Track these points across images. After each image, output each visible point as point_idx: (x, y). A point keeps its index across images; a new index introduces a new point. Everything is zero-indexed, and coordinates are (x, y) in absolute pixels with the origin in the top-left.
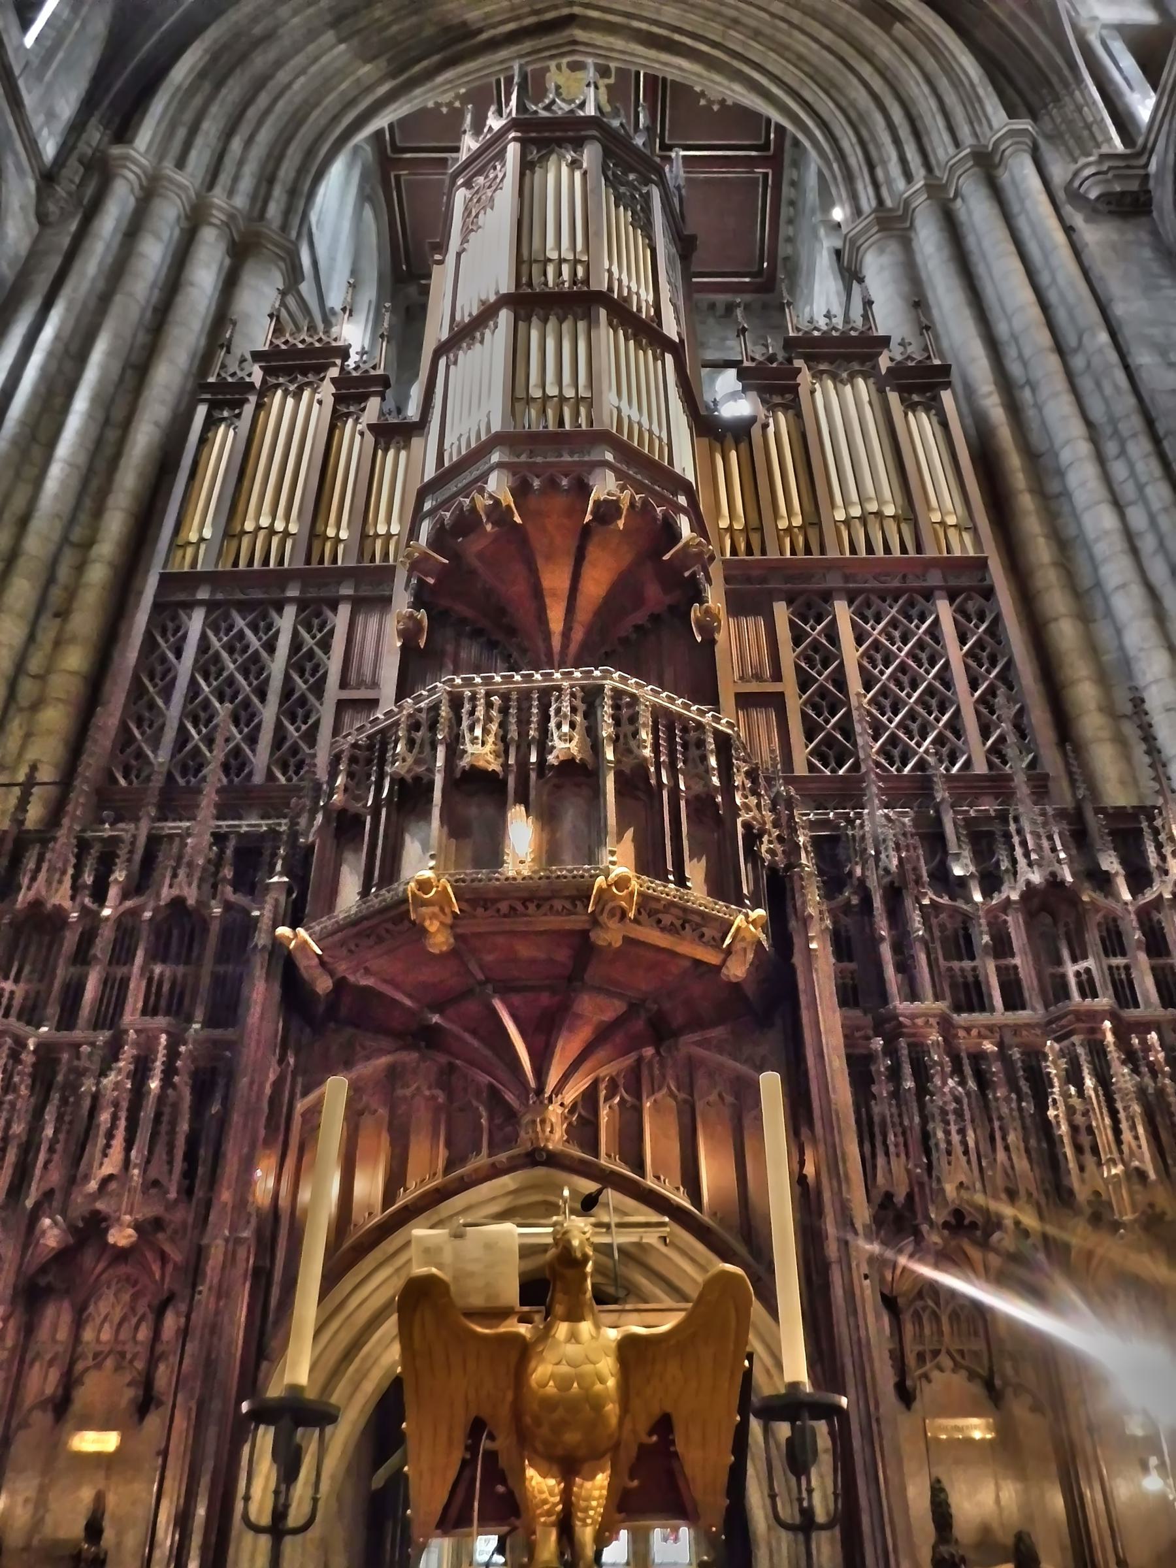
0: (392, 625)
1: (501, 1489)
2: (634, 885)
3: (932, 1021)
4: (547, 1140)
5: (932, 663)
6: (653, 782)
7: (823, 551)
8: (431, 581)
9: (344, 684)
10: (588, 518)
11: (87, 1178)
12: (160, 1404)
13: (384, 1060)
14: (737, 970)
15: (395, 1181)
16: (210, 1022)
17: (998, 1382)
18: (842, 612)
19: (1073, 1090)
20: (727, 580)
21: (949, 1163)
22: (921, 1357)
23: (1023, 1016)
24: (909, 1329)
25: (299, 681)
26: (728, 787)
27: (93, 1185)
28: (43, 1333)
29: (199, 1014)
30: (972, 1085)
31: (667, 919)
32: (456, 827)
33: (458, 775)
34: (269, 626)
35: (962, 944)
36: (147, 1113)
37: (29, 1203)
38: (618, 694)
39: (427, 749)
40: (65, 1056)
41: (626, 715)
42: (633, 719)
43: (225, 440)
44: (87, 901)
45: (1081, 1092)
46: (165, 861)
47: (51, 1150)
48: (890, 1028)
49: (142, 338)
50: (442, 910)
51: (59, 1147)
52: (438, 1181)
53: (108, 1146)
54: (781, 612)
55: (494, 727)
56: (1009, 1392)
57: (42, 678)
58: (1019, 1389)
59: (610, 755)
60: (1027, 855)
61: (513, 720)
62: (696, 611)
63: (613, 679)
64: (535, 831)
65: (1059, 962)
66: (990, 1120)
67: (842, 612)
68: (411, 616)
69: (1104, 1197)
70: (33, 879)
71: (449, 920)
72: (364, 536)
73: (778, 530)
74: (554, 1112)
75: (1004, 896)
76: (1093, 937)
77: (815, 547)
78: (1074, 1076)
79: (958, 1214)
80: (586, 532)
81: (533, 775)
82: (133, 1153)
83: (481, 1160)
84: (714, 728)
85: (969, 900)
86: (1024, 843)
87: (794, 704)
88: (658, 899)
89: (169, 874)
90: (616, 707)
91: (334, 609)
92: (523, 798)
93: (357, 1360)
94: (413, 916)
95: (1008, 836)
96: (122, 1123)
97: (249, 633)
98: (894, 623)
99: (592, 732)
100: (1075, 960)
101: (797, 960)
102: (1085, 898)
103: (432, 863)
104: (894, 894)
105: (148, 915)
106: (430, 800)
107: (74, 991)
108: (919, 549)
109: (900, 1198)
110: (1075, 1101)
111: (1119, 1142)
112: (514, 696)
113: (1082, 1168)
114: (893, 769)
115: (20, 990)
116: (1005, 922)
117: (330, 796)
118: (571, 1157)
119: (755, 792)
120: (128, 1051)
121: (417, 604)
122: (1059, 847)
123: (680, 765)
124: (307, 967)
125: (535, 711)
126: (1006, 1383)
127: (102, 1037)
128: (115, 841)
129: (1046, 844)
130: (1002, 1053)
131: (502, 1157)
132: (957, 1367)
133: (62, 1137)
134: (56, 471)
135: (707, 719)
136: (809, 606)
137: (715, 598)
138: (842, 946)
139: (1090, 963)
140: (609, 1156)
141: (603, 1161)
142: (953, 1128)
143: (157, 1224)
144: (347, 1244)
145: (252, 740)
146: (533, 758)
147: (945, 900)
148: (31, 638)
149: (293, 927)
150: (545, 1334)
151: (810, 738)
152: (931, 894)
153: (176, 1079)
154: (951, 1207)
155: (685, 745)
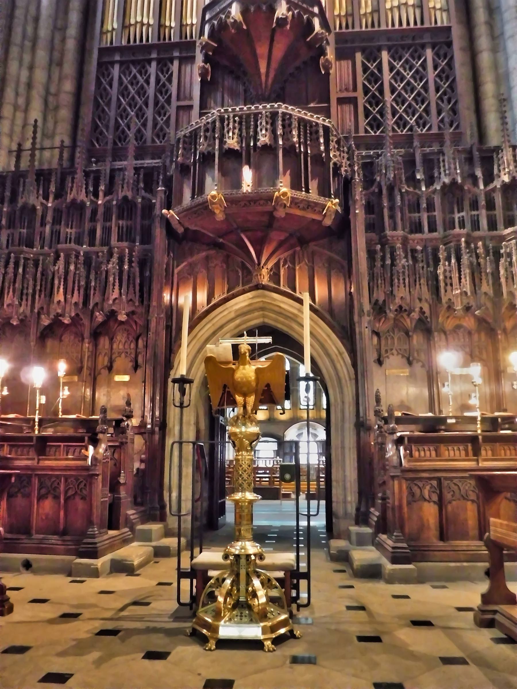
0: (196, 72)
1: (232, 398)
2: (289, 195)
3: (400, 238)
4: (262, 281)
5: (421, 80)
6: (297, 151)
7: (379, 26)
8: (211, 53)
9: (178, 99)
10: (274, 25)
11: (108, 299)
12: (141, 367)
13: (204, 254)
14: (328, 222)
15: (210, 296)
16: (142, 242)
17: (411, 359)
18: (385, 56)
19: (447, 263)
20: (337, 42)
21: (398, 290)
22: (386, 351)
23: (435, 234)
24: (383, 342)
25: (161, 98)
26: (327, 150)
27: (111, 302)
28: (100, 346)
29: (138, 238)
30: (411, 262)
31: (301, 206)
32: (223, 172)
33: (224, 151)
34: (146, 72)
35: (416, 207)
36: (125, 277)
37: (91, 307)
38: (284, 114)
39: (212, 139)
40: (94, 257)
41: (287, 126)
42: (290, 125)
44: (92, 198)
45: (450, 265)
46: (118, 180)
47: (95, 289)
48: (383, 241)
50: (221, 206)
51: (97, 289)
52: (225, 295)
53: (114, 288)
54: (359, 57)
55: (236, 131)
56: (415, 362)
57: (56, 95)
58: (418, 361)
59: (281, 142)
60: (445, 171)
61: (244, 127)
62: (322, 60)
63: (283, 108)
64: (253, 174)
65: (453, 212)
66: (415, 275)
67: (385, 56)
68: (204, 67)
69: (452, 301)
70: (71, 190)
71: (223, 209)
72: (181, 25)
73: (360, 15)
74: (264, 271)
75: (434, 187)
76: (466, 204)
77: (376, 24)
78: (448, 259)
79: (401, 307)
80: (274, 31)
81: (252, 151)
82: (122, 291)
83: (240, 288)
84: (323, 125)
85: (420, 189)
86: (444, 166)
87: (361, 101)
88: (298, 199)
89: (120, 186)
90: (283, 120)
91: (172, 63)
92: (248, 163)
93: (202, 353)
94: (210, 207)
95: (439, 162)
96: (117, 281)
97: (138, 76)
98: (407, 61)
99: (274, 132)
100: (459, 212)
101: (351, 217)
102: (466, 188)
103: (216, 188)
104: (391, 189)
105: (114, 203)
106: (214, 161)
107: (93, 232)
108: (422, 23)
109: (381, 302)
110: (447, 268)
111: (460, 282)
112: (244, 117)
113: (446, 291)
114: (399, 131)
115: (73, 231)
116: (434, 198)
117: (177, 157)
118: (271, 287)
119: (338, 149)
120: (116, 256)
121: (206, 61)
122: (458, 167)
123: (308, 142)
124: (175, 225)
125: (252, 123)
126: (414, 359)
127: (105, 249)
128: (98, 171)
129: (452, 166)
130: (425, 247)
131: (247, 287)
132: (398, 354)
133: (98, 285)
135: (320, 121)
136: (371, 53)
137: (330, 54)
138: (369, 208)
139: (463, 214)
140: (284, 286)
141: (282, 288)
142: (401, 278)
143: (133, 313)
144: (196, 317)
145: (144, 125)
146: (252, 144)
147: (411, 189)
148: (49, 77)
149: (168, 209)
150: (238, 368)
151: (367, 117)
152: (406, 187)
153: (133, 264)
154: (398, 305)
155: (311, 134)
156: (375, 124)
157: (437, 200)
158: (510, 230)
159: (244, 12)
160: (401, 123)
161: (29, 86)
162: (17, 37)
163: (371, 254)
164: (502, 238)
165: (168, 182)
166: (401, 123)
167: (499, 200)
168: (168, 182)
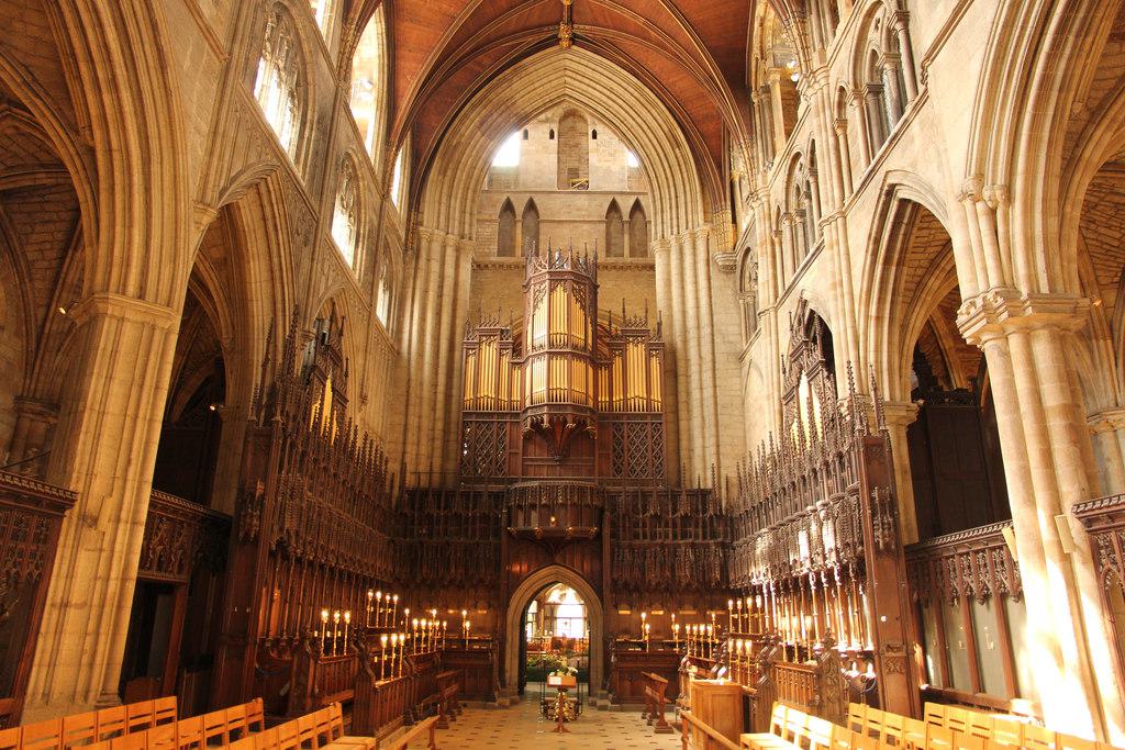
15: (529, 567)
23: (646, 541)
43: (472, 360)
107: (467, 530)
138: (613, 524)
156: (619, 471)
158: (682, 542)
159: (550, 422)
164: (679, 545)
165: (509, 508)
167: (679, 521)
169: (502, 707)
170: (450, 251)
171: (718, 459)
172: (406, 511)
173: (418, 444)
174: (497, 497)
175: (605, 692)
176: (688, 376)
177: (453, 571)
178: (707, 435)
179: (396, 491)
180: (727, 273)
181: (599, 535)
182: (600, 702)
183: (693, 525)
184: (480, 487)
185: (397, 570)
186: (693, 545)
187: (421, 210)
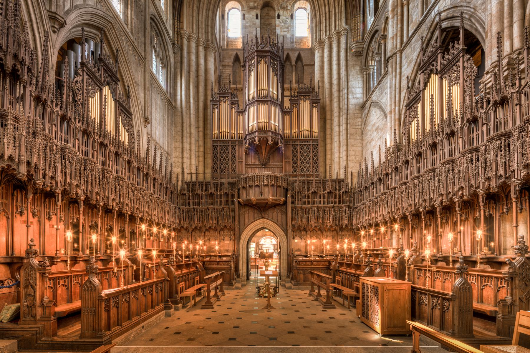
18: (299, 147)
49: (196, 79)
76: (318, 196)
107: (217, 202)
134: (192, 116)
138: (292, 197)
157: (310, 195)
160: (302, 170)
161: (190, 150)
162: (185, 134)
163: (292, 210)
165: (239, 190)
166: (302, 170)
167: (326, 195)
168: (239, 190)
169: (237, 288)
170: (201, 49)
171: (347, 163)
172: (185, 192)
173: (190, 159)
174: (232, 184)
175: (289, 280)
176: (332, 120)
177: (211, 222)
178: (341, 151)
179: (180, 183)
180: (357, 56)
181: (285, 203)
182: (288, 285)
183: (334, 196)
184: (223, 180)
185: (182, 222)
186: (333, 207)
187: (181, 21)
